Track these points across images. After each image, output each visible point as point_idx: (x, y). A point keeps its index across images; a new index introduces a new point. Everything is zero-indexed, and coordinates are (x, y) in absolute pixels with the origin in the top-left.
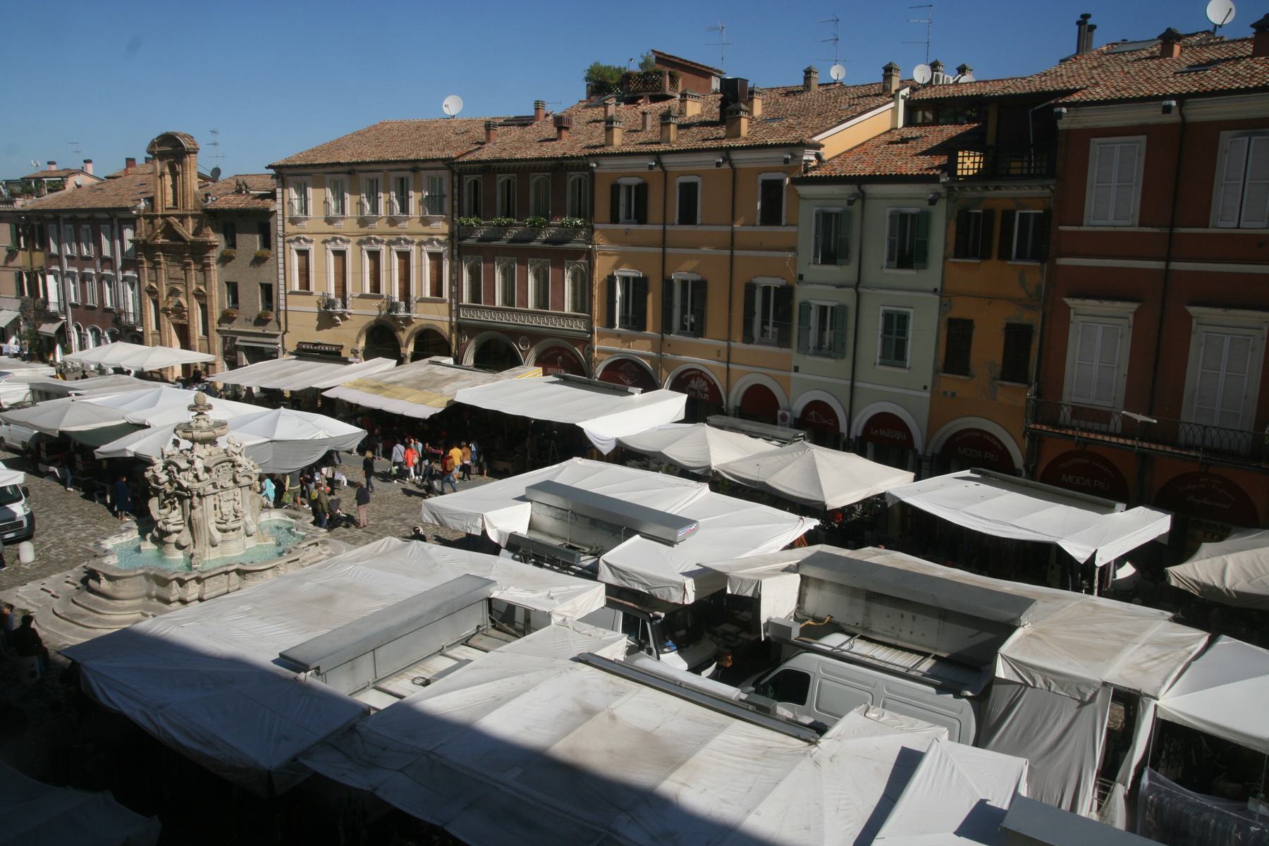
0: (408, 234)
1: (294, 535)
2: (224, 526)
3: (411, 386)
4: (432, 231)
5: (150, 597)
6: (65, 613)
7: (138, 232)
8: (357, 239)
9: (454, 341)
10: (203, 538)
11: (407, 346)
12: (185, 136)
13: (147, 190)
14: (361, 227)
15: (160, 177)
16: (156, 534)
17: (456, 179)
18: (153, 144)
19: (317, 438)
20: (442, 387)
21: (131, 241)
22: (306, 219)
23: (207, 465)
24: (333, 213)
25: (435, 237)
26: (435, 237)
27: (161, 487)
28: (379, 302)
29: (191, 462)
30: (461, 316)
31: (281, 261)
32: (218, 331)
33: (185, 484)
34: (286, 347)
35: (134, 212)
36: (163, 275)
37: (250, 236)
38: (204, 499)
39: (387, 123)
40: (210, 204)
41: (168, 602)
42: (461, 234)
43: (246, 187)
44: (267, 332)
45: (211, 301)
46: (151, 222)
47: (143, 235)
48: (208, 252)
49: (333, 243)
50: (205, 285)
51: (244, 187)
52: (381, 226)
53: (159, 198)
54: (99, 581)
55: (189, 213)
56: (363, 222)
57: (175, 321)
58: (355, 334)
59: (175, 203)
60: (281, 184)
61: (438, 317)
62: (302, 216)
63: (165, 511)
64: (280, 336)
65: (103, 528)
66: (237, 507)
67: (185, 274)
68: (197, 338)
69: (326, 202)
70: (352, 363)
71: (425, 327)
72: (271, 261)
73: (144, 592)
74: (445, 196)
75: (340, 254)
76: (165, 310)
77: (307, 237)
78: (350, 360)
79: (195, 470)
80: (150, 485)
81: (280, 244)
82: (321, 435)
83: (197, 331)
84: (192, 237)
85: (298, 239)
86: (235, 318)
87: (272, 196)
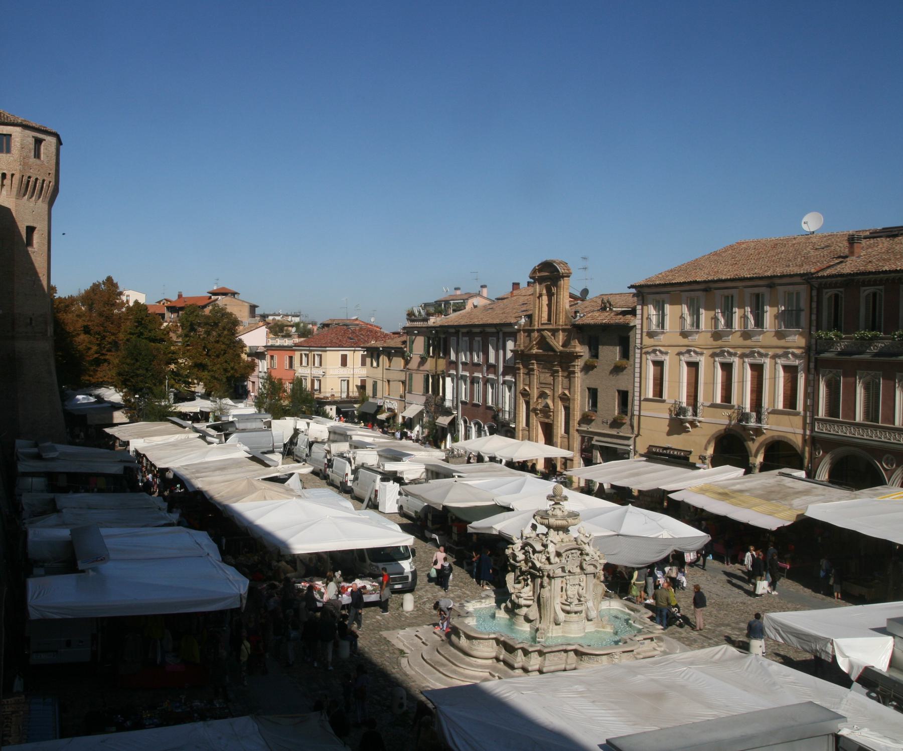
0: (762, 347)
2: (567, 608)
7: (517, 343)
8: (711, 351)
9: (807, 455)
10: (549, 616)
11: (756, 456)
14: (715, 340)
17: (814, 293)
19: (661, 537)
20: (793, 499)
21: (512, 351)
22: (663, 333)
23: (559, 550)
24: (688, 327)
25: (790, 350)
26: (790, 350)
28: (729, 412)
29: (545, 546)
30: (816, 430)
31: (637, 370)
32: (577, 430)
33: (538, 565)
36: (535, 380)
37: (611, 348)
38: (553, 580)
39: (743, 243)
40: (578, 320)
42: (818, 347)
43: (610, 305)
44: (621, 434)
45: (574, 404)
46: (529, 336)
47: (522, 346)
48: (574, 361)
49: (687, 355)
50: (569, 390)
51: (608, 305)
52: (734, 339)
53: (537, 315)
55: (560, 328)
56: (717, 336)
57: (543, 420)
58: (704, 441)
59: (549, 319)
60: (641, 302)
62: (660, 330)
63: (519, 586)
64: (633, 439)
66: (581, 591)
67: (554, 380)
68: (559, 435)
69: (682, 317)
70: (699, 468)
71: (776, 438)
74: (803, 310)
75: (693, 366)
76: (535, 410)
77: (662, 349)
78: (698, 465)
79: (548, 553)
81: (638, 356)
82: (665, 535)
83: (560, 429)
84: (561, 348)
85: (654, 351)
86: (593, 420)
87: (633, 312)
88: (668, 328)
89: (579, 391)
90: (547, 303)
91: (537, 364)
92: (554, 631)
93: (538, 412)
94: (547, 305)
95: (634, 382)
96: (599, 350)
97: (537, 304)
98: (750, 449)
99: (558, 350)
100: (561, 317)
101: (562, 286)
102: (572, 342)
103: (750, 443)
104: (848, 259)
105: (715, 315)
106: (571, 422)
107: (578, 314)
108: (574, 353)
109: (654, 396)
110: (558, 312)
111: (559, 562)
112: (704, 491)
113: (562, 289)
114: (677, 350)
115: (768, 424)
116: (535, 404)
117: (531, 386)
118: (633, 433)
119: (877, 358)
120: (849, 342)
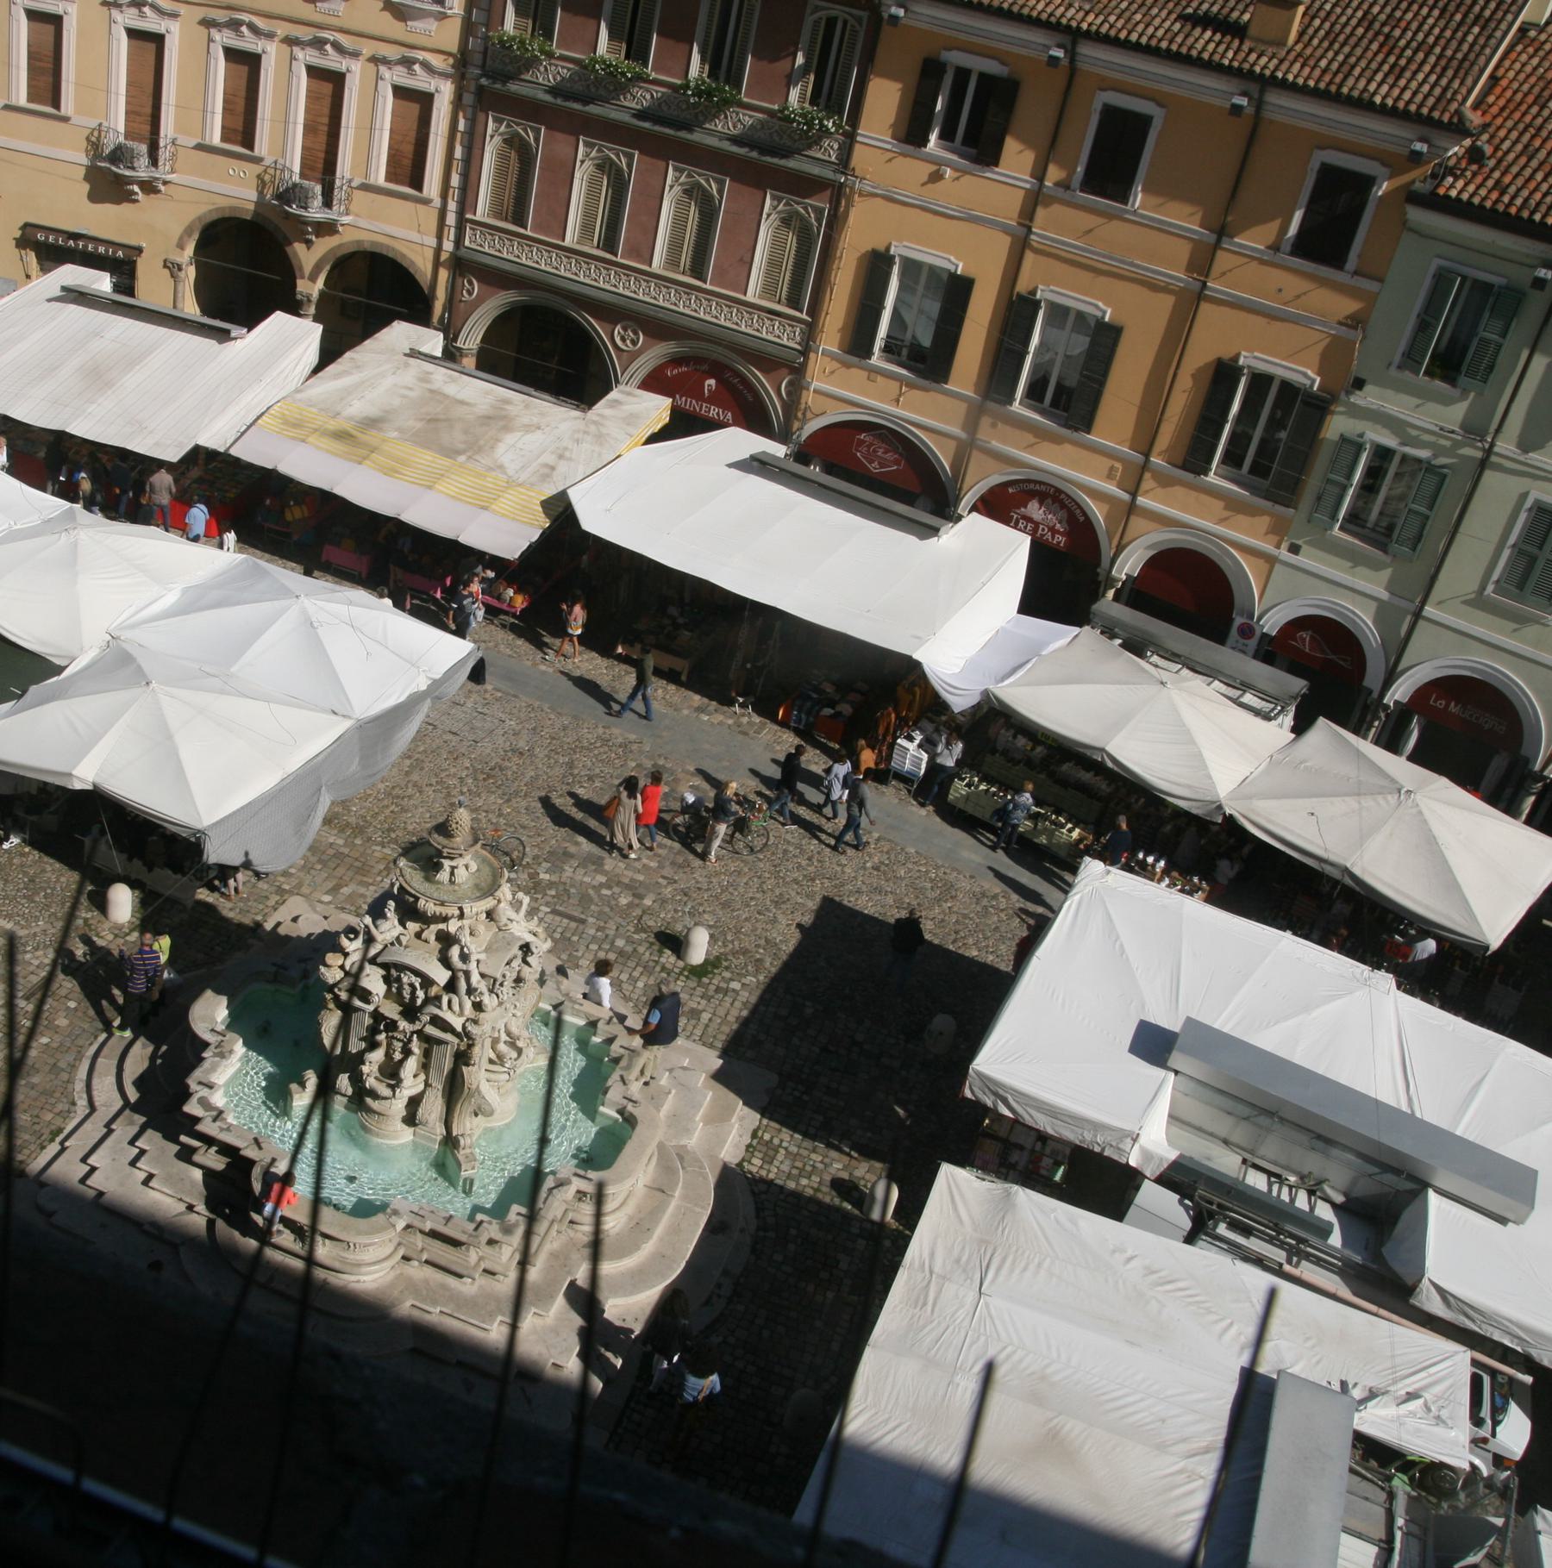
8: (201, 13)
11: (313, 278)
25: (420, 55)
30: (467, 243)
49: (134, 11)
58: (177, 230)
71: (368, 247)
103: (299, 247)
120: (569, 69)
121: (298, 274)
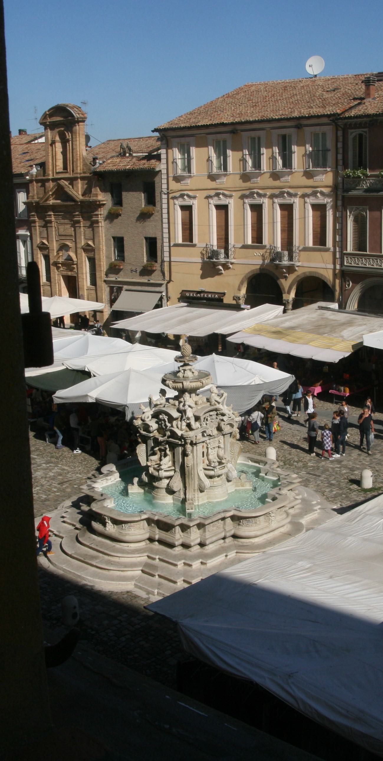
0: (291, 187)
1: (263, 479)
2: (211, 473)
3: (310, 331)
4: (316, 184)
5: (151, 540)
6: (75, 553)
7: (30, 195)
8: (240, 194)
9: (337, 288)
10: (192, 485)
11: (289, 293)
12: (73, 108)
13: (32, 157)
14: (244, 181)
15: (51, 145)
16: (145, 478)
17: (340, 133)
18: (45, 116)
19: (253, 383)
20: (341, 331)
21: (25, 203)
22: (190, 177)
23: (197, 414)
24: (215, 171)
25: (319, 189)
26: (319, 189)
27: (151, 435)
28: (262, 252)
29: (182, 412)
30: (345, 264)
31: (165, 216)
32: (105, 281)
33: (179, 433)
34: (169, 295)
35: (28, 177)
36: (54, 233)
37: (135, 194)
38: (195, 447)
39: (252, 86)
40: (99, 167)
41: (171, 546)
42: (345, 186)
43: (130, 150)
44: (152, 281)
45: (99, 254)
46: (43, 185)
47: (36, 197)
48: (96, 210)
49: (216, 198)
50: (93, 240)
51: (127, 150)
52: (265, 180)
53: (50, 164)
54: (104, 524)
55: (79, 176)
56: (245, 177)
57: (65, 273)
58: (237, 283)
59: (65, 167)
60: (165, 146)
61: (323, 265)
62: (186, 174)
63: (155, 458)
64: (164, 286)
65: (66, 468)
66: (221, 453)
67: (75, 230)
68: (85, 288)
69: (209, 160)
70: (243, 309)
72: (156, 216)
73: (147, 536)
74: (329, 150)
75: (223, 209)
76: (56, 264)
77: (190, 193)
78: (242, 306)
79: (188, 419)
80: (139, 432)
82: (257, 381)
83: (85, 281)
84: (81, 197)
85: (182, 196)
86: (122, 269)
87: (158, 158)
88: (195, 172)
89: (104, 241)
90: (61, 150)
91: (54, 215)
92: (200, 499)
93: (60, 265)
94: (62, 153)
95: (162, 228)
96: (123, 197)
97: (50, 152)
98: (283, 286)
99: (78, 200)
100: (79, 164)
101: (78, 132)
102: (93, 190)
103: (283, 281)
104: (365, 101)
105: (243, 157)
106: (97, 274)
107: (97, 161)
108: (96, 201)
109: (183, 241)
110: (75, 159)
111: (200, 427)
112: (258, 331)
113: (78, 135)
114: (206, 193)
115: (299, 262)
116: (57, 258)
117: (50, 239)
118: (164, 279)
119: (368, 194)
121: (283, 292)
